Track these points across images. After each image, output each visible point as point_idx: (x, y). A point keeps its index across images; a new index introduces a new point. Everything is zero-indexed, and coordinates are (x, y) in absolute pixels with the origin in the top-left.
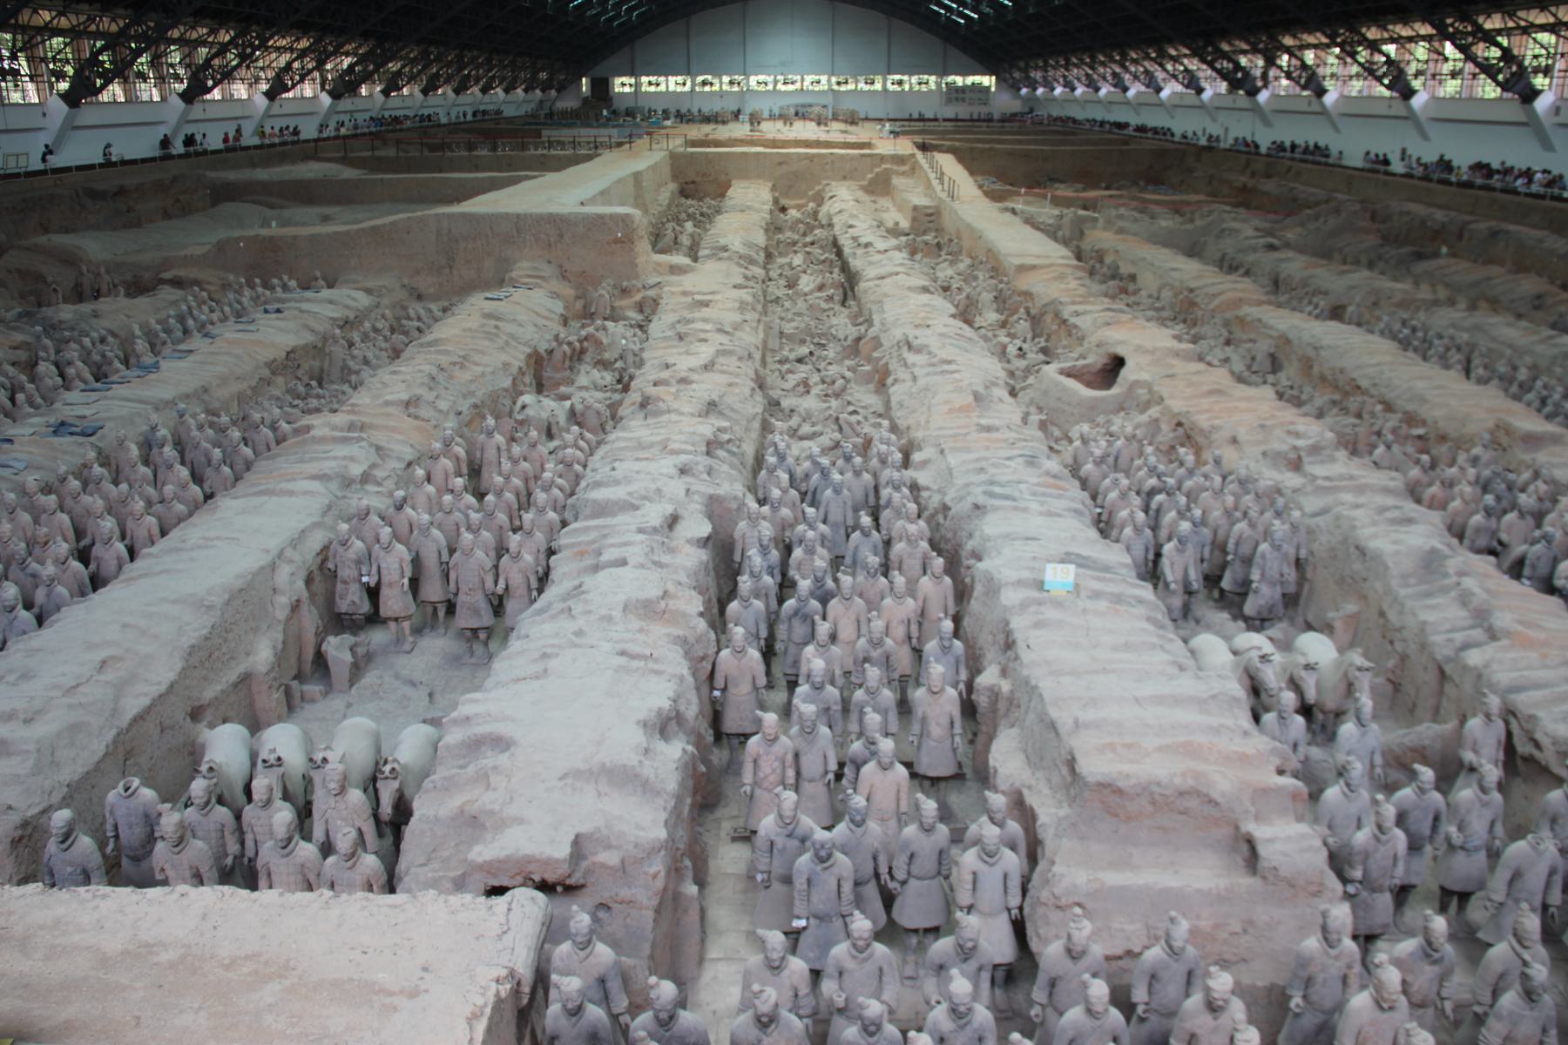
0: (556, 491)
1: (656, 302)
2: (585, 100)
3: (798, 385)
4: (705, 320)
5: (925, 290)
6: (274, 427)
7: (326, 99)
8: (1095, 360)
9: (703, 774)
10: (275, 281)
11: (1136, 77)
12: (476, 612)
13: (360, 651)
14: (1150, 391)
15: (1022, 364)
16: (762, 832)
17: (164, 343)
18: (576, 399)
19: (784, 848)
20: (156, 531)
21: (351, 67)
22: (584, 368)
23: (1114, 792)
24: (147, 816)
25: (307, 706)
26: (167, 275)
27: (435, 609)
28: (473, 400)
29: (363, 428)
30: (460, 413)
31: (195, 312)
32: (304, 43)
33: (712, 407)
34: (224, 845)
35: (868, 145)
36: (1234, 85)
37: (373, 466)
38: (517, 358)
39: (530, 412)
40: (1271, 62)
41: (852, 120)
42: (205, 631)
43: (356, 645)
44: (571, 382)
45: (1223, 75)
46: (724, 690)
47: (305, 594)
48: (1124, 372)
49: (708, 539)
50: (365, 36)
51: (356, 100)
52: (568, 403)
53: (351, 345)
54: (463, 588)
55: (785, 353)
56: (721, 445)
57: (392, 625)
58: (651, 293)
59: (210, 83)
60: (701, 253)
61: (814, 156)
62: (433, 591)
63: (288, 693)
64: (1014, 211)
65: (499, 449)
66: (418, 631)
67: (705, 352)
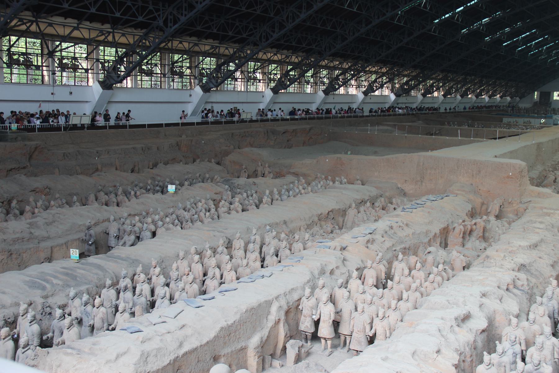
0: (418, 294)
2: (536, 103)
4: (541, 223)
6: (304, 244)
7: (393, 97)
10: (337, 179)
13: (303, 350)
17: (277, 200)
21: (407, 83)
22: (473, 238)
25: (271, 369)
26: (292, 171)
27: (346, 337)
28: (403, 246)
30: (395, 250)
32: (384, 70)
33: (522, 267)
37: (337, 267)
38: (436, 228)
42: (230, 323)
43: (302, 346)
47: (283, 318)
49: (483, 331)
50: (415, 67)
51: (408, 98)
54: (355, 330)
56: (515, 287)
57: (323, 341)
58: (524, 206)
59: (337, 87)
62: (344, 330)
63: (263, 361)
66: (335, 347)
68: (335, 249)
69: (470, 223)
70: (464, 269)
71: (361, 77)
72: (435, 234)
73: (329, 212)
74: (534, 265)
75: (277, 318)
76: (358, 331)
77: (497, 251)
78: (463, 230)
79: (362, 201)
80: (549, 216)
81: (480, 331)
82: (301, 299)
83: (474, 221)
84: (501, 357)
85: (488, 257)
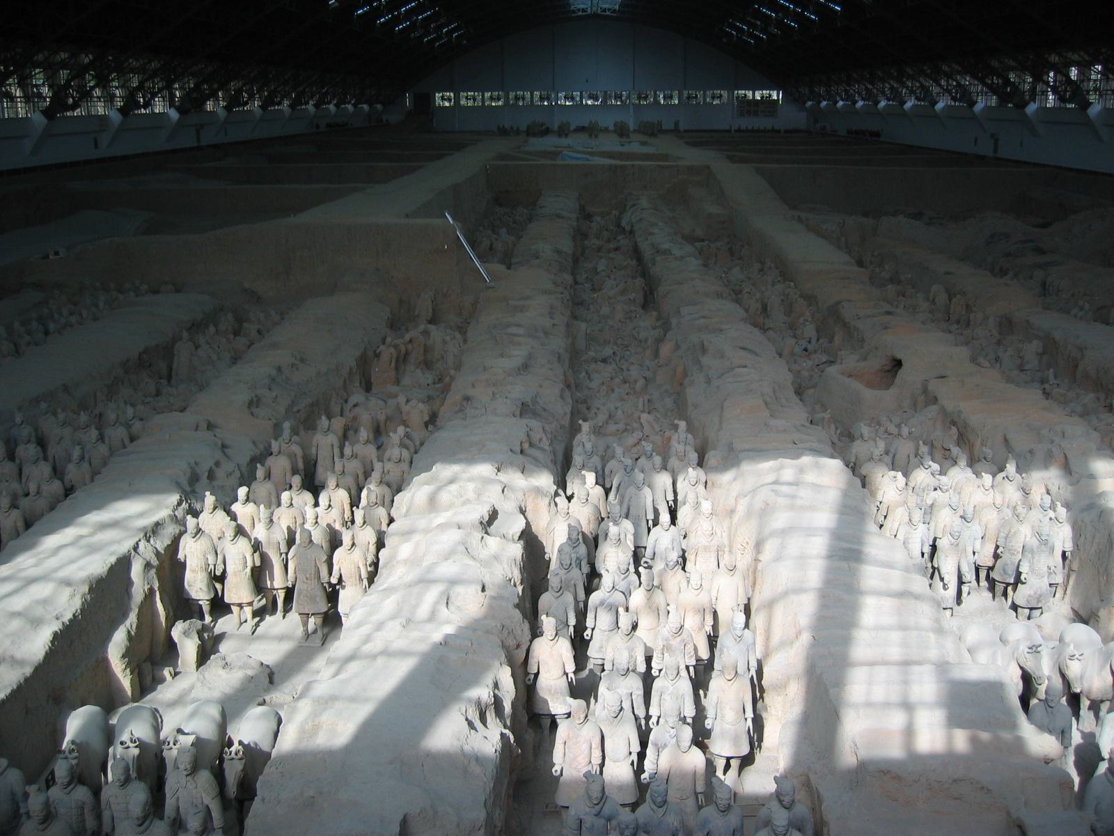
1: (474, 305)
3: (603, 383)
4: (518, 325)
5: (719, 296)
7: (174, 115)
8: (877, 362)
9: (518, 756)
11: (912, 92)
12: (312, 599)
14: (925, 391)
15: (810, 363)
16: (572, 811)
18: (402, 399)
19: (593, 826)
20: (20, 524)
21: (197, 86)
23: (894, 778)
24: (13, 794)
29: (210, 426)
30: (298, 411)
31: (56, 316)
34: (84, 821)
35: (665, 157)
36: (1003, 99)
37: (217, 464)
39: (357, 410)
40: (1039, 78)
41: (651, 130)
44: (397, 382)
45: (993, 89)
46: (537, 675)
47: (156, 585)
48: (901, 372)
52: (392, 402)
53: (197, 347)
55: (592, 354)
57: (235, 609)
60: (514, 261)
61: (616, 167)
64: (800, 220)
65: (332, 446)
66: (260, 614)
67: (518, 355)
68: (197, 429)
69: (402, 341)
70: (427, 427)
71: (113, 80)
72: (351, 369)
73: (140, 353)
74: (538, 400)
75: (147, 587)
76: (307, 579)
77: (473, 386)
78: (395, 356)
79: (193, 325)
80: (521, 311)
81: (518, 534)
82: (176, 542)
83: (407, 337)
84: (568, 572)
85: (467, 399)
